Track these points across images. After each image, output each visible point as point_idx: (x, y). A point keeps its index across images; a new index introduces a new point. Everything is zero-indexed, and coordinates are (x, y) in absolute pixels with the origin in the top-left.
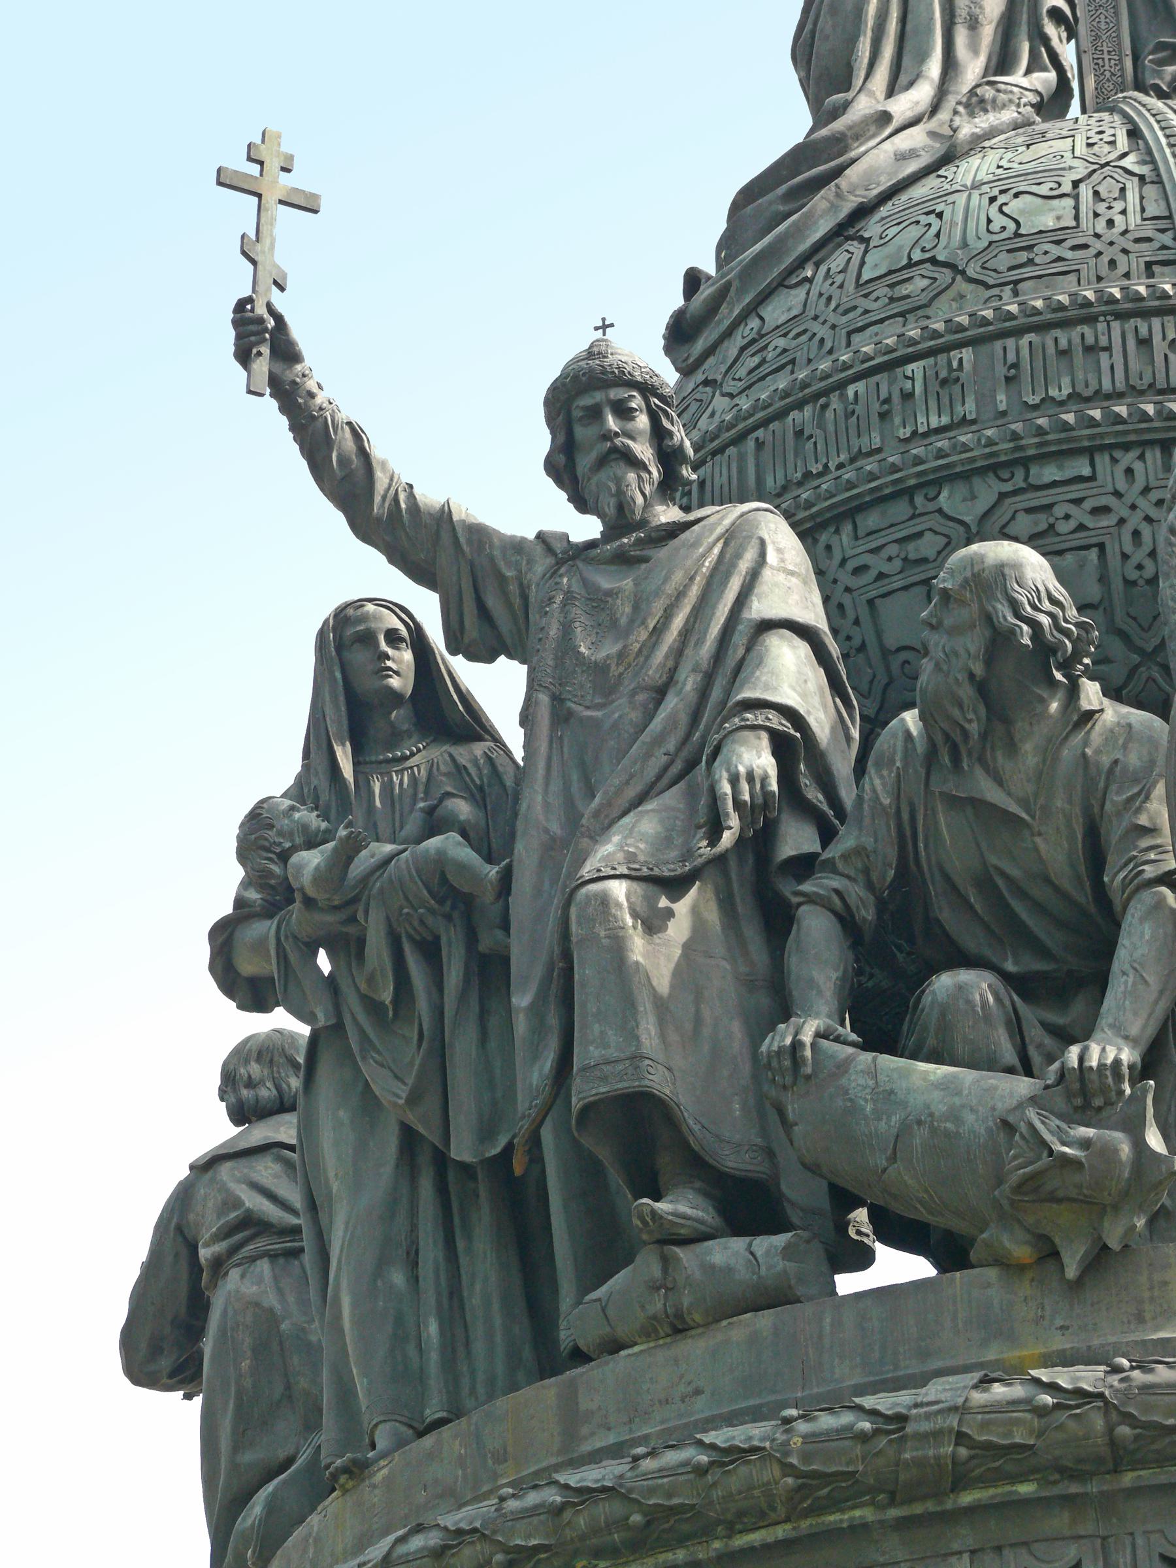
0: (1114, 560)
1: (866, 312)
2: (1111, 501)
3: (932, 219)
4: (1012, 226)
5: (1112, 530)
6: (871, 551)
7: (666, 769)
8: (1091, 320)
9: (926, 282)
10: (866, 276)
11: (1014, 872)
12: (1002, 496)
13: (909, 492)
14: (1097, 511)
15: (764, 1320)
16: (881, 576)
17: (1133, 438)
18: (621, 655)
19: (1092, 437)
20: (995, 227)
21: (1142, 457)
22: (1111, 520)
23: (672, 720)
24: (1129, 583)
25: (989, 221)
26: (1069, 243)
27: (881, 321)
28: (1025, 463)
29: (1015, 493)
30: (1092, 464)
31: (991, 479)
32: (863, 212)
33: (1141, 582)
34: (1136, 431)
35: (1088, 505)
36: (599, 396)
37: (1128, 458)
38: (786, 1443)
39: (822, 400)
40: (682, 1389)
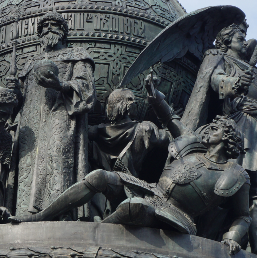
0: (111, 68)
2: (113, 55)
5: (111, 61)
14: (109, 56)
21: (121, 47)
22: (112, 59)
24: (113, 74)
30: (110, 46)
33: (116, 74)
35: (108, 54)
37: (118, 47)
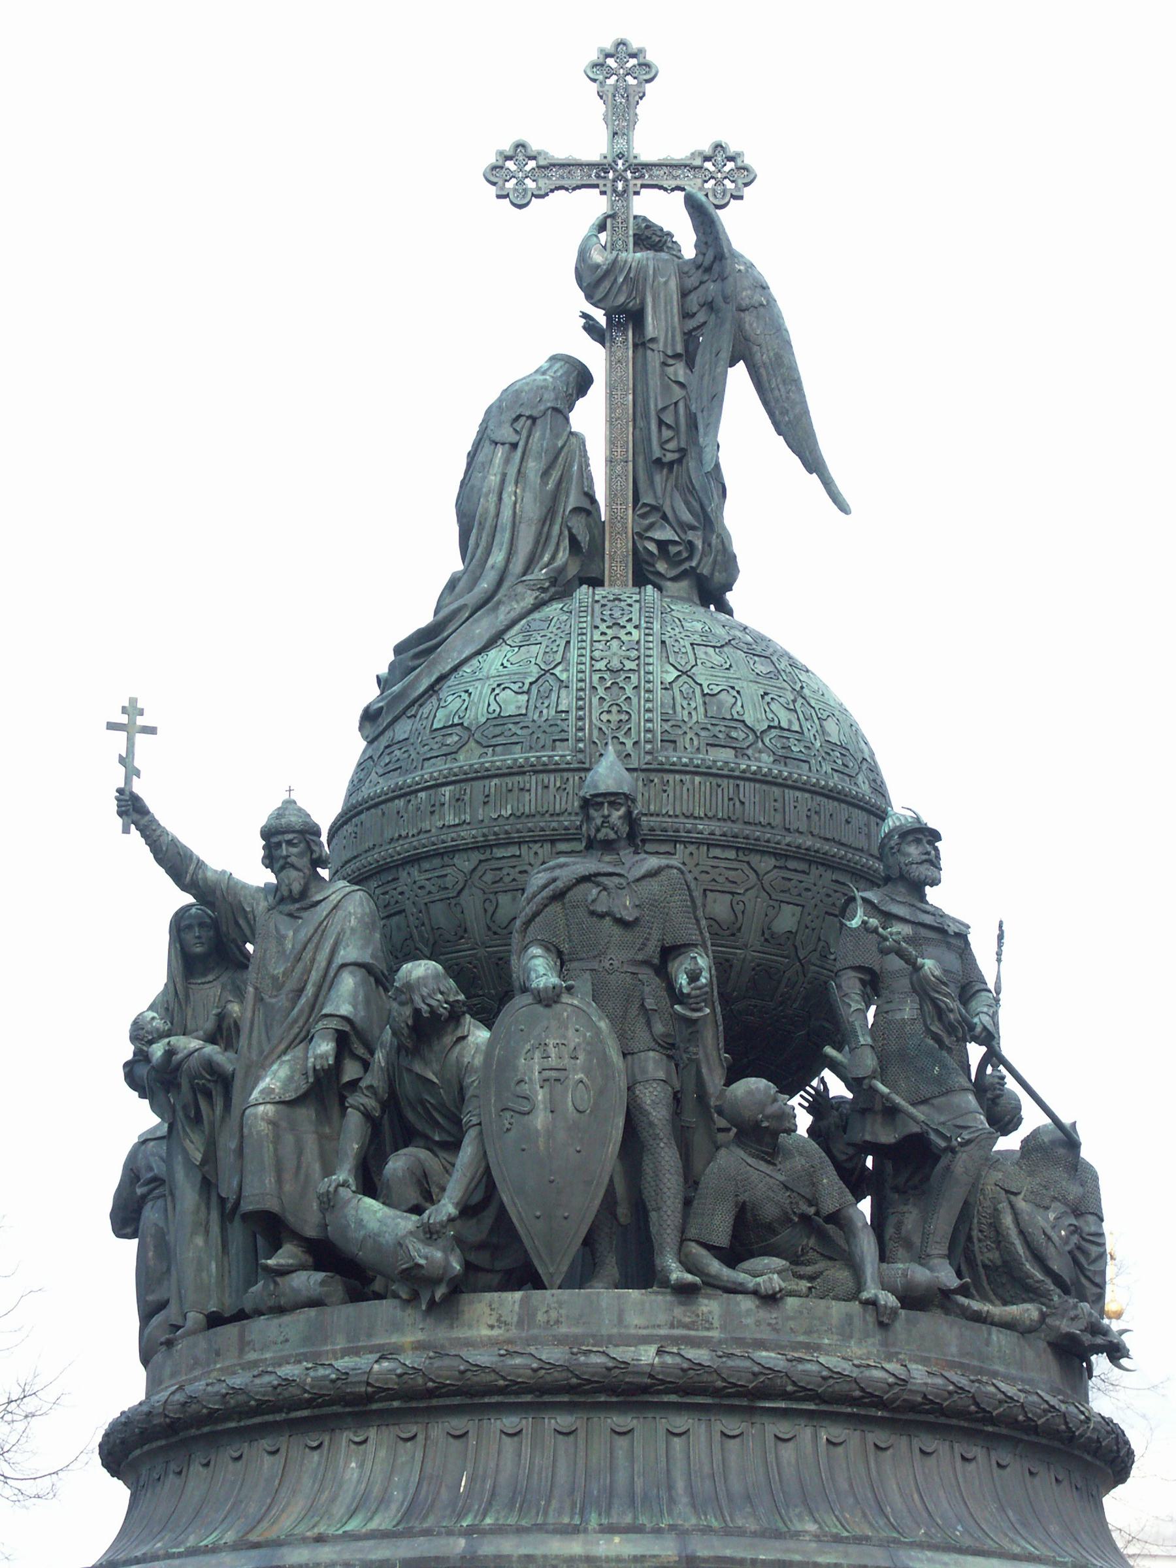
1: (432, 749)
3: (465, 696)
4: (498, 710)
6: (427, 880)
7: (298, 1034)
8: (524, 773)
9: (456, 738)
10: (435, 727)
11: (432, 1101)
12: (481, 861)
13: (442, 854)
14: (520, 872)
15: (312, 1312)
16: (430, 893)
17: (537, 839)
18: (284, 973)
19: (520, 837)
20: (491, 710)
23: (301, 1011)
25: (489, 705)
26: (521, 725)
27: (437, 757)
28: (491, 846)
29: (486, 860)
30: (520, 848)
31: (476, 853)
32: (443, 678)
34: (539, 836)
35: (517, 869)
36: (280, 838)
37: (536, 847)
38: (305, 1380)
39: (408, 798)
40: (281, 1338)
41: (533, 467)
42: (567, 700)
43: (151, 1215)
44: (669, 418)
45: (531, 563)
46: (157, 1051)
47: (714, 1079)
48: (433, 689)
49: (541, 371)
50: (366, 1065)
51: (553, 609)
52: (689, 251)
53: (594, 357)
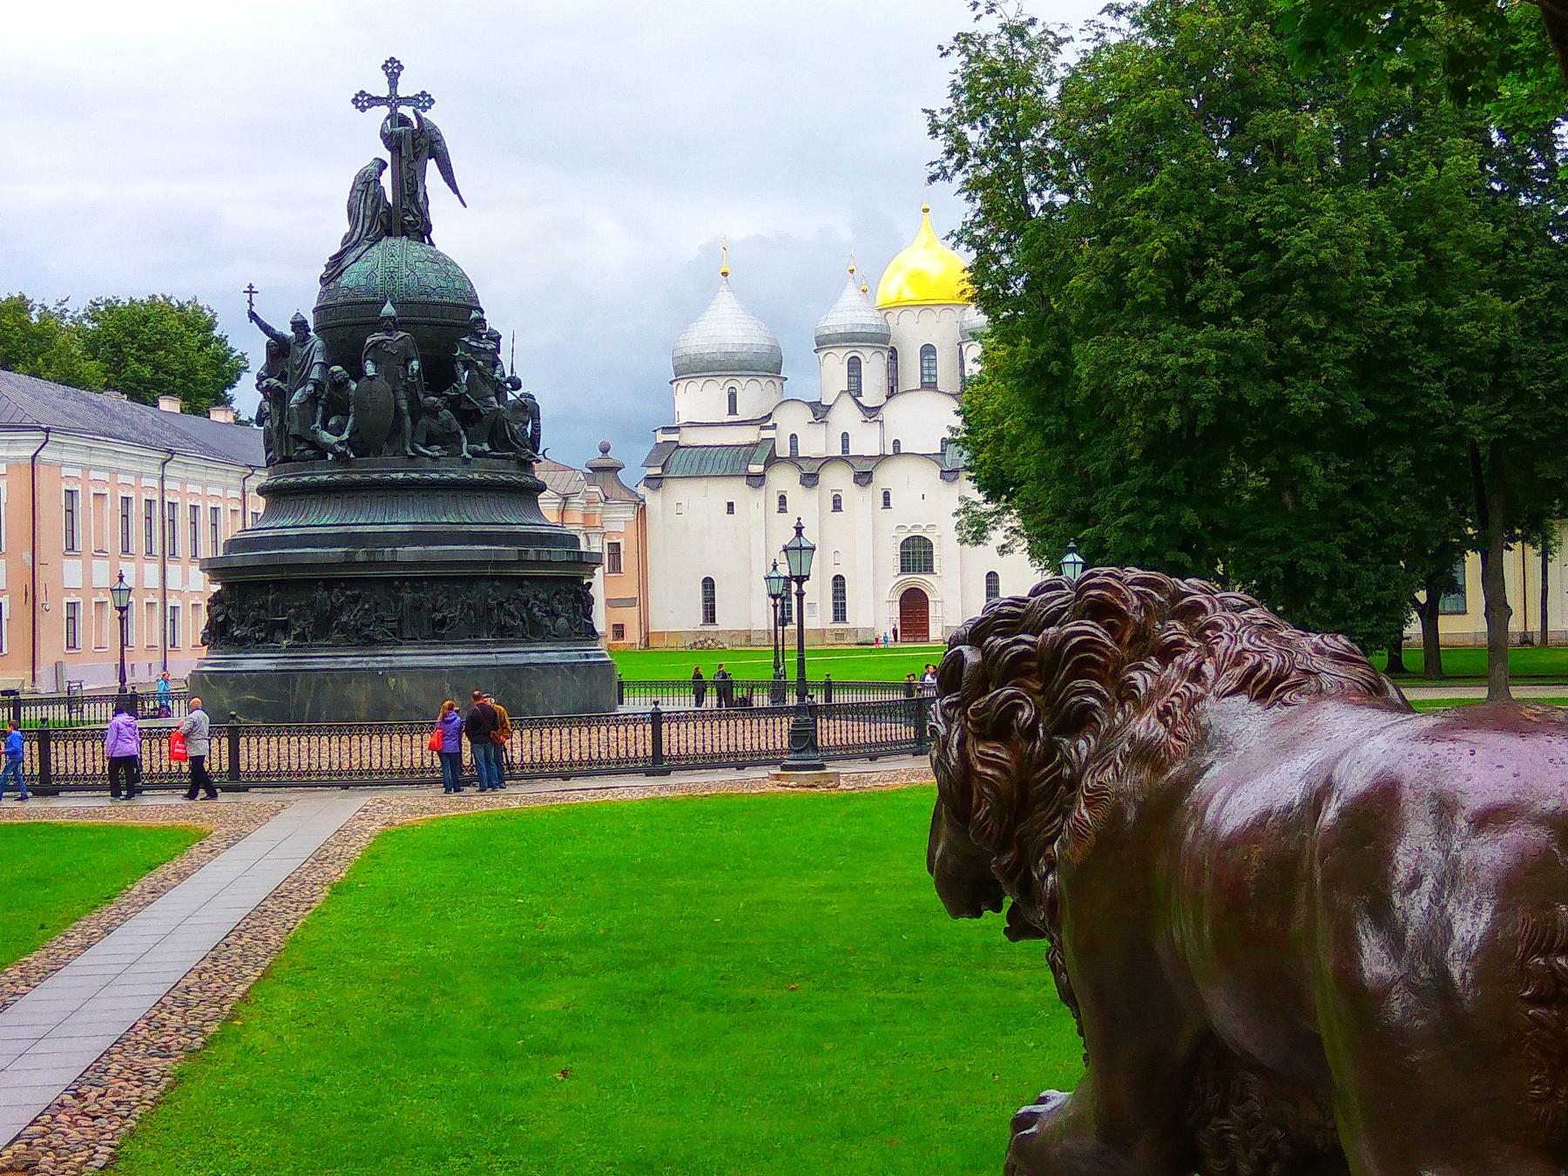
41: (369, 201)
42: (378, 282)
43: (267, 423)
44: (410, 181)
45: (369, 230)
46: (264, 383)
47: (421, 396)
48: (340, 274)
49: (371, 164)
50: (323, 392)
51: (374, 248)
52: (416, 127)
53: (387, 156)
